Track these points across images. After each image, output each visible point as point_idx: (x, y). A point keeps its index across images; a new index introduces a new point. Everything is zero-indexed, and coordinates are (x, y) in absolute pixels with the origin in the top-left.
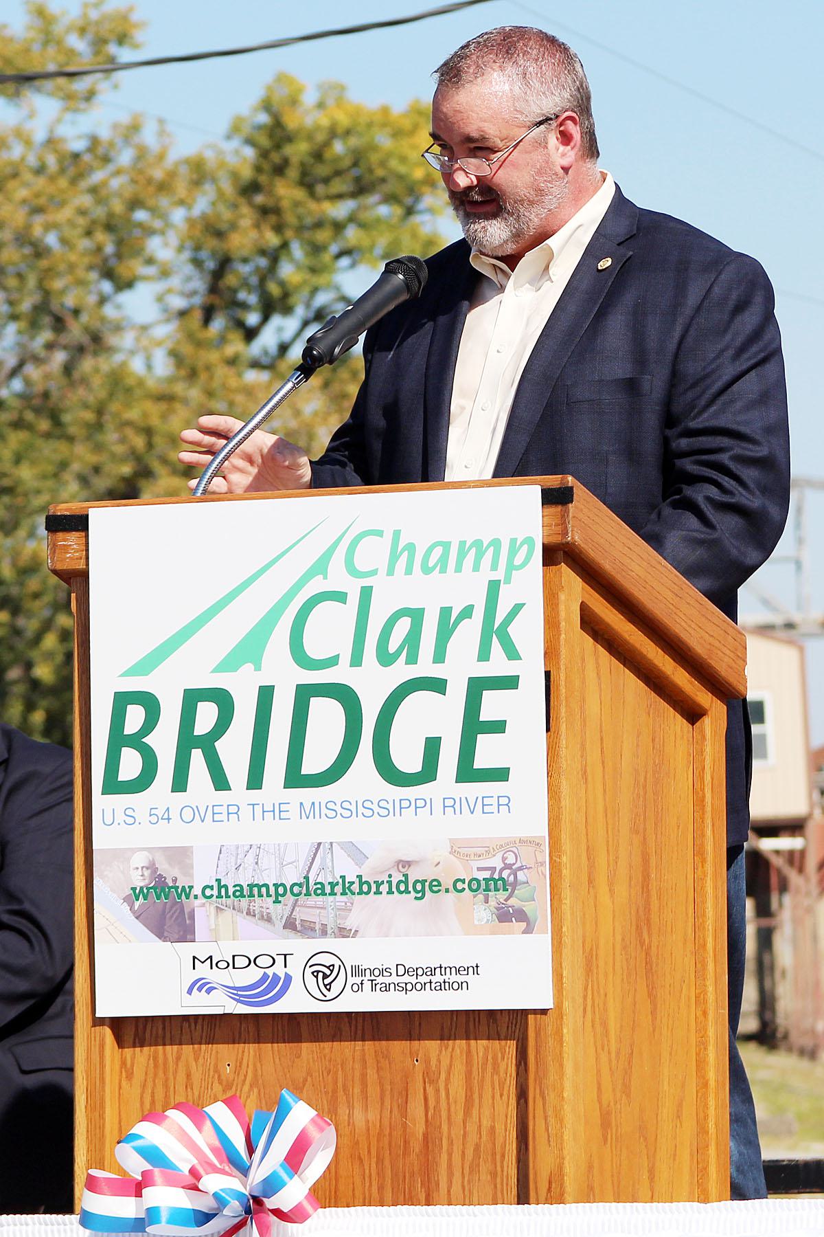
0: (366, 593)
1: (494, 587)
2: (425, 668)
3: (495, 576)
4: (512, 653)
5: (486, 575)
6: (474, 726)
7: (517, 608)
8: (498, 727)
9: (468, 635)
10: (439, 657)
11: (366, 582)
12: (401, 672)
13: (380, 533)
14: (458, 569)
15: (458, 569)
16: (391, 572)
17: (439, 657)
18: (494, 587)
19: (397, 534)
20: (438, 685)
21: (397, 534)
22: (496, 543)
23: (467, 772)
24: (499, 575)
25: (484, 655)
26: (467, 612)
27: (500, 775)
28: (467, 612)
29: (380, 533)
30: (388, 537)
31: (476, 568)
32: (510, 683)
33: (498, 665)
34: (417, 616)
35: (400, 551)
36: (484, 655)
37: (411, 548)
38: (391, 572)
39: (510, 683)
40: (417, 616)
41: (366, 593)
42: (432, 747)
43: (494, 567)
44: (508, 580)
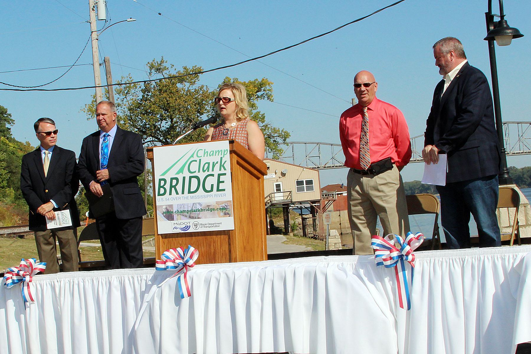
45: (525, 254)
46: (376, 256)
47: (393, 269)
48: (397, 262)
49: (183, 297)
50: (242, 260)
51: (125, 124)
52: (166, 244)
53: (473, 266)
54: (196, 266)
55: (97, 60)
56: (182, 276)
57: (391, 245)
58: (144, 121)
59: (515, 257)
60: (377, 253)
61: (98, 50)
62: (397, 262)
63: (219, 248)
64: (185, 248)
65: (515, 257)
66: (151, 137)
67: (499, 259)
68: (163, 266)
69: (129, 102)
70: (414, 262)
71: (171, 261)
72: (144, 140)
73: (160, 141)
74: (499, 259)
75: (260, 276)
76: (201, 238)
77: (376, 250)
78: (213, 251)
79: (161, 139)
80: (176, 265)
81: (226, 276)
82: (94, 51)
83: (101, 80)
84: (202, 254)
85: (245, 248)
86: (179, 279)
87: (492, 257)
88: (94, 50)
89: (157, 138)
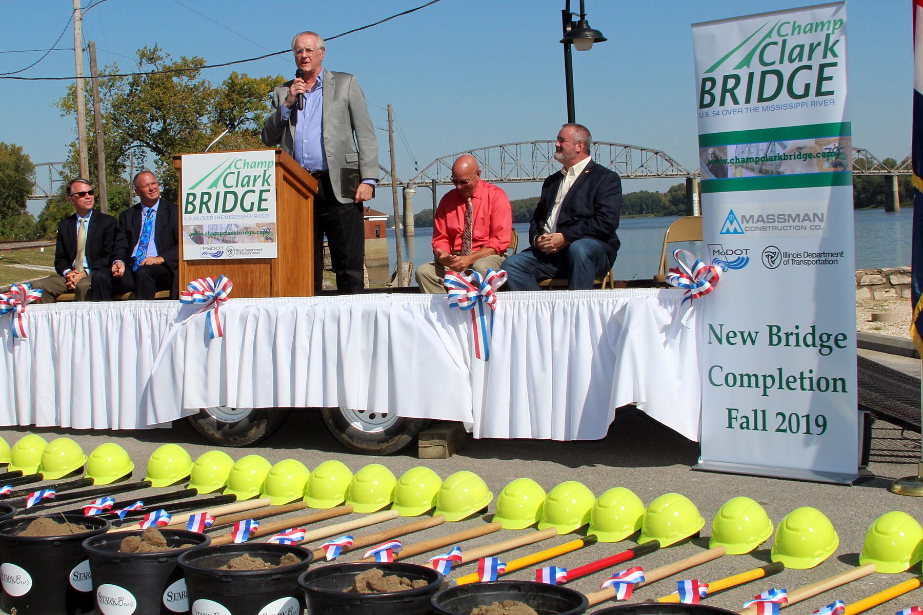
1: (828, 36)
3: (828, 32)
4: (835, 55)
5: (825, 32)
7: (837, 41)
18: (828, 36)
22: (829, 22)
24: (830, 31)
31: (822, 30)
32: (835, 64)
39: (835, 64)
43: (828, 29)
44: (833, 33)
45: (627, 300)
46: (450, 296)
47: (469, 312)
48: (474, 304)
49: (213, 337)
50: (285, 295)
51: (108, 124)
52: (192, 272)
53: (565, 311)
54: (230, 301)
55: (79, 44)
56: (213, 311)
57: (467, 283)
58: (131, 121)
59: (615, 302)
60: (451, 292)
61: (81, 32)
62: (474, 304)
63: (258, 280)
64: (215, 277)
65: (615, 302)
66: (138, 141)
67: (596, 304)
68: (189, 299)
69: (114, 97)
70: (494, 305)
71: (199, 292)
72: (129, 145)
73: (148, 145)
74: (596, 304)
75: (308, 315)
76: (235, 266)
77: (451, 289)
78: (250, 282)
79: (150, 143)
80: (206, 298)
81: (266, 314)
82: (76, 33)
83: (82, 67)
84: (237, 286)
85: (288, 280)
86: (209, 314)
87: (587, 302)
88: (77, 31)
89: (146, 143)
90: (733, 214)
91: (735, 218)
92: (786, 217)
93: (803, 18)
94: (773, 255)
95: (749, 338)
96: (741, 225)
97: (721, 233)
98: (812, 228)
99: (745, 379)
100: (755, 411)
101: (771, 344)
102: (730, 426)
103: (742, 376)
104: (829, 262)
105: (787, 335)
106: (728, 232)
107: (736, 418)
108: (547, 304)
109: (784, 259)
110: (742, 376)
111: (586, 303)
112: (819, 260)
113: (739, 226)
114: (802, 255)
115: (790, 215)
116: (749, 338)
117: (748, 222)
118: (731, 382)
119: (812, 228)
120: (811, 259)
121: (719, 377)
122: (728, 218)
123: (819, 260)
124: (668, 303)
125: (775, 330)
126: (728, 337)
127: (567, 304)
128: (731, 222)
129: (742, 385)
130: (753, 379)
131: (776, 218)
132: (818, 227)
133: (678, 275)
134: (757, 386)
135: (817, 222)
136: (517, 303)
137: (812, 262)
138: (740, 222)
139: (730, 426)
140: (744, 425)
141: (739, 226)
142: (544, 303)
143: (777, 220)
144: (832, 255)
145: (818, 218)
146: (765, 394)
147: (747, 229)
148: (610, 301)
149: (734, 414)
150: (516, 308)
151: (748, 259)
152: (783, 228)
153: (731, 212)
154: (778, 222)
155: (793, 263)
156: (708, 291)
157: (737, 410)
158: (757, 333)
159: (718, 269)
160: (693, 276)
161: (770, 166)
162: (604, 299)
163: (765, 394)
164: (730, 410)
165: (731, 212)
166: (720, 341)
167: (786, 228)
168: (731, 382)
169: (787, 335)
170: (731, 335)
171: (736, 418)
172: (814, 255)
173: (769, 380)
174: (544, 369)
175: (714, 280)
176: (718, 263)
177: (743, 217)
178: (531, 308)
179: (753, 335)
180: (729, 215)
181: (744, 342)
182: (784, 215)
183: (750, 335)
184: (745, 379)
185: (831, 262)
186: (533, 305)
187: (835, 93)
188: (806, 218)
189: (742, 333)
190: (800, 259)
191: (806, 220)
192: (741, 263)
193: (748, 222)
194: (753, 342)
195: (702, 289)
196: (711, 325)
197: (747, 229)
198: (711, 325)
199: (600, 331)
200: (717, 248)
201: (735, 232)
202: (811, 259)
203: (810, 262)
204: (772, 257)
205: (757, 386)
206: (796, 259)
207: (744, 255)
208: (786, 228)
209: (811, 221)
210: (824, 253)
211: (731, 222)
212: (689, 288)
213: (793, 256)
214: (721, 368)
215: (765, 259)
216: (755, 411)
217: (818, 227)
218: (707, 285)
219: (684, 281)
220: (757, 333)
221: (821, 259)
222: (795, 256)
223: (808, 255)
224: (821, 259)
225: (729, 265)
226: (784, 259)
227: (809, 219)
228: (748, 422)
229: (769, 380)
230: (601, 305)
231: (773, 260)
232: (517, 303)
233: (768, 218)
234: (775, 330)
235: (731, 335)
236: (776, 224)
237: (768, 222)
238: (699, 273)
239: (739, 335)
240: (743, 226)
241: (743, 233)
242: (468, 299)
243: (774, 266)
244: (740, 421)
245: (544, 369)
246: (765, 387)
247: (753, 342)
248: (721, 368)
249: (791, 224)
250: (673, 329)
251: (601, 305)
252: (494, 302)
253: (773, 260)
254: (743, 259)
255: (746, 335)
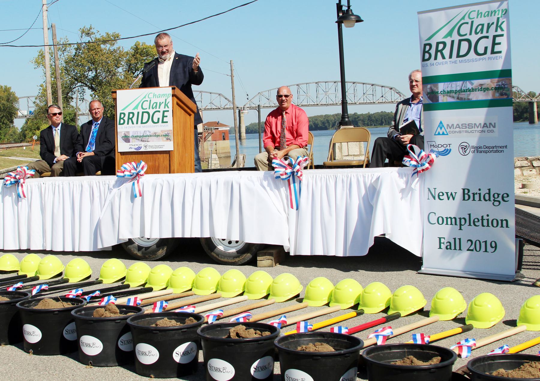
0: (472, 22)
1: (498, 19)
2: (485, 34)
3: (498, 16)
5: (497, 16)
6: (494, 44)
8: (499, 44)
9: (493, 27)
10: (487, 32)
11: (472, 20)
12: (480, 35)
13: (475, 11)
14: (491, 16)
15: (491, 16)
16: (477, 18)
17: (487, 32)
18: (498, 19)
19: (478, 11)
20: (487, 37)
21: (478, 11)
23: (493, 52)
25: (496, 31)
26: (493, 23)
27: (500, 52)
28: (493, 23)
29: (475, 11)
30: (477, 12)
31: (494, 15)
33: (499, 32)
34: (483, 25)
35: (479, 14)
36: (496, 31)
37: (481, 13)
38: (477, 18)
40: (483, 25)
41: (472, 22)
42: (486, 48)
43: (498, 15)
90: (442, 124)
91: (443, 126)
92: (473, 125)
93: (484, 8)
94: (465, 148)
95: (451, 196)
96: (447, 130)
97: (435, 135)
98: (489, 131)
99: (449, 220)
100: (455, 239)
101: (464, 199)
102: (440, 248)
103: (447, 218)
104: (499, 152)
105: (474, 194)
106: (439, 134)
107: (444, 243)
108: (332, 176)
109: (472, 150)
110: (447, 218)
111: (355, 176)
112: (493, 150)
113: (446, 131)
114: (483, 147)
115: (475, 124)
116: (451, 196)
117: (450, 128)
118: (440, 222)
119: (489, 131)
120: (488, 150)
121: (433, 219)
122: (439, 126)
123: (493, 150)
124: (404, 176)
125: (466, 191)
126: (439, 196)
127: (344, 176)
128: (441, 128)
129: (447, 224)
130: (453, 220)
131: (467, 125)
132: (492, 131)
133: (410, 159)
134: (456, 224)
135: (492, 128)
136: (315, 176)
137: (488, 152)
138: (446, 128)
139: (440, 248)
140: (449, 247)
141: (446, 131)
142: (331, 176)
143: (467, 127)
144: (501, 147)
145: (492, 125)
146: (460, 229)
147: (450, 132)
148: (370, 175)
149: (442, 240)
150: (314, 179)
151: (450, 150)
152: (471, 132)
153: (441, 123)
154: (468, 128)
155: (477, 152)
156: (427, 169)
157: (444, 238)
158: (456, 193)
159: (433, 156)
160: (419, 160)
161: (464, 95)
162: (366, 174)
163: (460, 229)
164: (440, 238)
165: (441, 123)
166: (434, 198)
167: (473, 132)
168: (440, 222)
169: (474, 194)
170: (441, 194)
171: (444, 243)
172: (490, 148)
173: (463, 221)
174: (330, 214)
175: (431, 162)
176: (433, 152)
177: (448, 125)
178: (323, 179)
179: (454, 194)
180: (440, 124)
181: (448, 199)
182: (472, 124)
183: (451, 194)
184: (449, 220)
185: (500, 151)
186: (324, 177)
187: (502, 52)
188: (485, 126)
189: (447, 193)
190: (481, 150)
191: (485, 127)
192: (446, 152)
193: (450, 128)
194: (454, 199)
195: (424, 167)
196: (429, 190)
197: (450, 132)
198: (429, 190)
199: (363, 192)
200: (433, 143)
201: (443, 134)
202: (488, 150)
203: (487, 152)
204: (465, 149)
205: (456, 224)
206: (479, 150)
207: (448, 148)
208: (473, 132)
209: (488, 128)
210: (496, 146)
211: (441, 128)
212: (416, 167)
213: (477, 148)
214: (435, 213)
215: (461, 150)
216: (455, 239)
217: (492, 131)
218: (427, 165)
219: (414, 163)
220: (456, 193)
221: (494, 150)
222: (478, 148)
223: (486, 147)
224: (494, 150)
225: (440, 154)
226: (472, 150)
227: (487, 127)
228: (450, 245)
229: (463, 221)
230: (364, 177)
231: (465, 150)
232: (315, 176)
233: (462, 126)
234: (466, 191)
235: (441, 194)
236: (467, 129)
237: (462, 128)
238: (422, 158)
239: (445, 194)
240: (448, 131)
241: (447, 134)
242: (286, 174)
243: (466, 154)
244: (446, 245)
245: (330, 214)
246: (461, 225)
247: (454, 199)
248: (435, 213)
249: (476, 129)
250: (406, 191)
251: (364, 177)
252: (301, 175)
253: (465, 150)
254: (448, 150)
255: (449, 194)
